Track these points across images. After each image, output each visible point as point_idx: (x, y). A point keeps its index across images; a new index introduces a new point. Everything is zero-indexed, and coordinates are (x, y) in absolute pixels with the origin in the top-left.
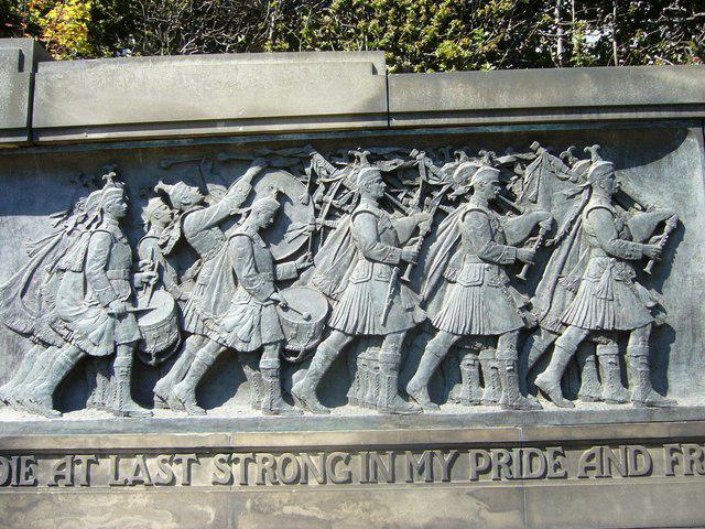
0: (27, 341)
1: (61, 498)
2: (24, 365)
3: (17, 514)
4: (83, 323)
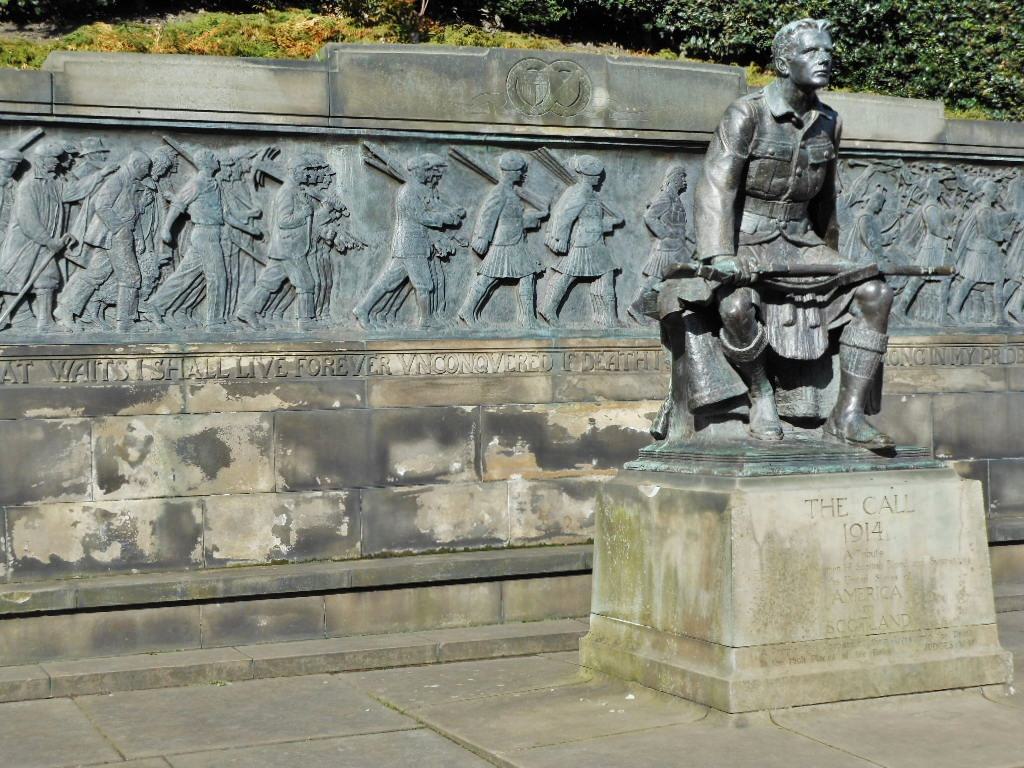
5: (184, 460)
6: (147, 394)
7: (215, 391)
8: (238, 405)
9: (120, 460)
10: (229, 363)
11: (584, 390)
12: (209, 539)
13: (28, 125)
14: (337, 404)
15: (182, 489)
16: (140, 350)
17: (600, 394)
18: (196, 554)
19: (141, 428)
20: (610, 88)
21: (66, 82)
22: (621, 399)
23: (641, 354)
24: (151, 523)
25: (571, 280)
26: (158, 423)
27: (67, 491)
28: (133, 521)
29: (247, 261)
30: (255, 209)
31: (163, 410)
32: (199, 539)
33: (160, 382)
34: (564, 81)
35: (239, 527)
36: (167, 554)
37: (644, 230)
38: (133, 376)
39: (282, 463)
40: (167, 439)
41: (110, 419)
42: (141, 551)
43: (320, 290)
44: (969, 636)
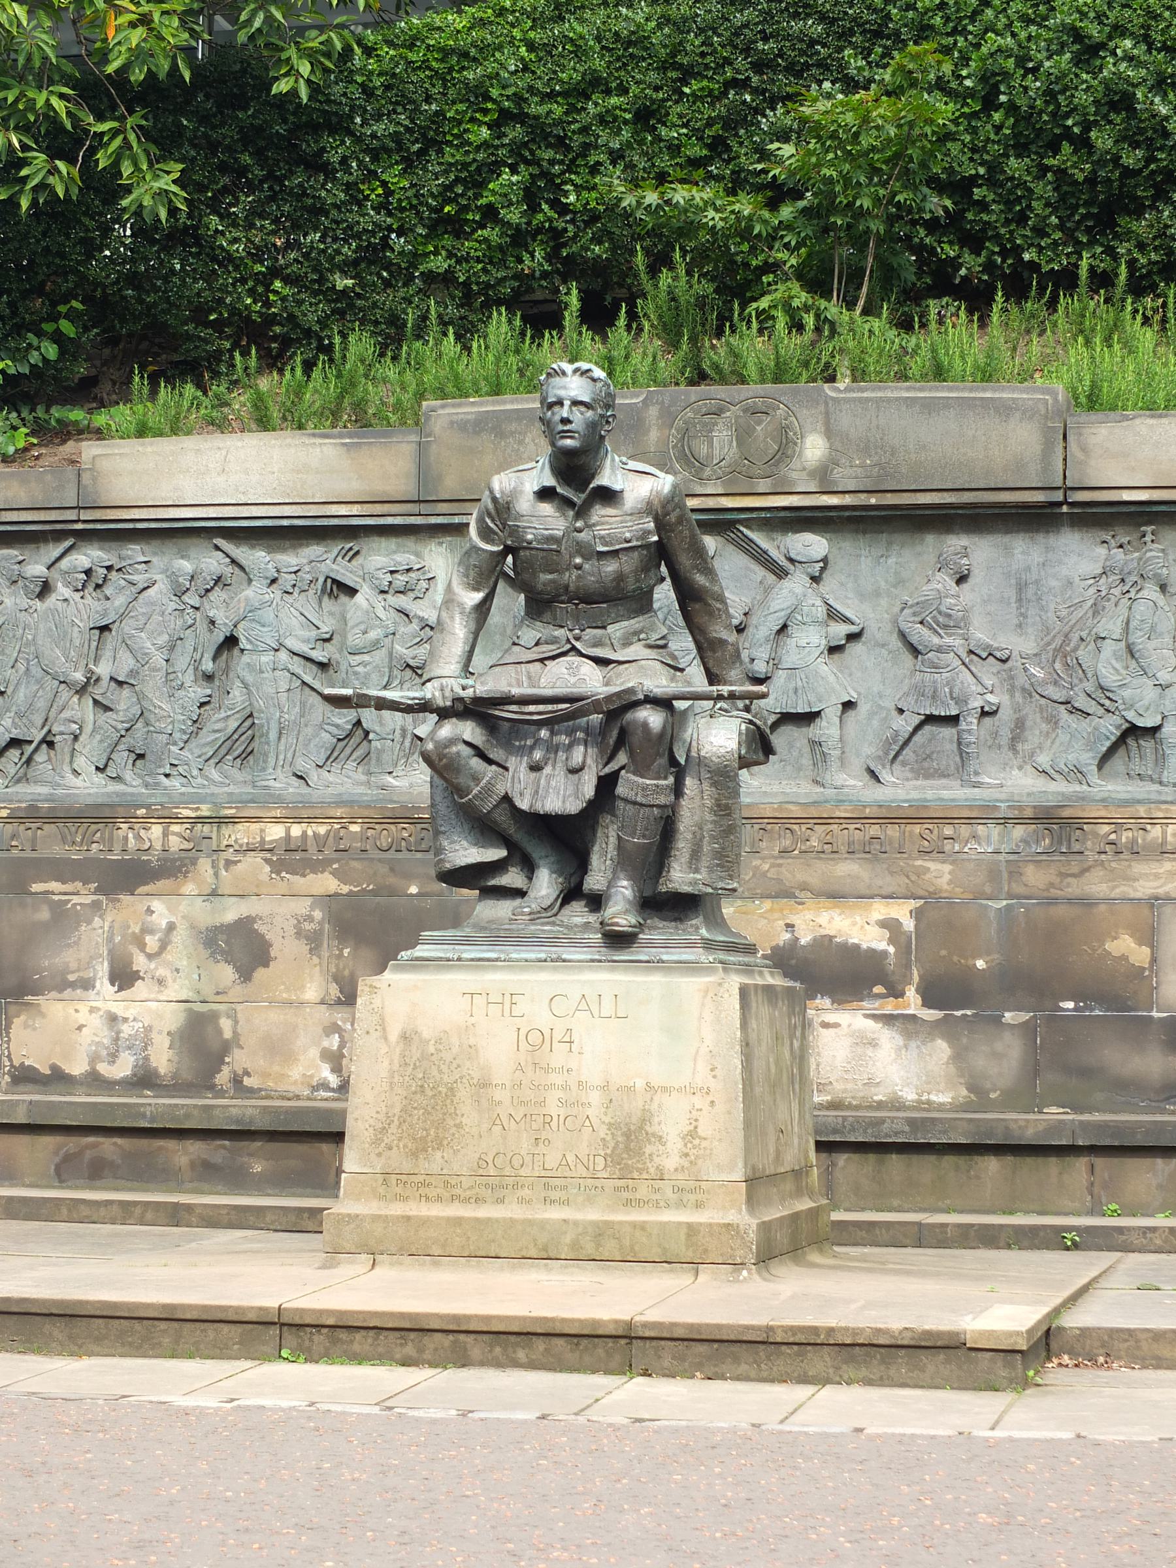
0: (1063, 707)
1: (1114, 865)
2: (1063, 737)
3: (1070, 880)
4: (1127, 693)
5: (212, 955)
6: (171, 868)
7: (254, 864)
8: (282, 887)
9: (135, 950)
10: (275, 832)
11: (779, 881)
12: (238, 1059)
13: (58, 536)
14: (413, 890)
15: (208, 991)
16: (166, 814)
17: (804, 887)
18: (223, 1078)
19: (161, 912)
20: (829, 433)
21: (94, 479)
22: (835, 895)
23: (874, 830)
24: (169, 1033)
26: (184, 906)
27: (73, 985)
28: (148, 1029)
29: (315, 699)
30: (324, 629)
31: (189, 888)
32: (227, 1060)
33: (190, 854)
34: (759, 428)
35: (279, 1048)
36: (187, 1075)
37: (895, 643)
38: (158, 846)
39: (337, 966)
40: (192, 927)
41: (125, 898)
42: (156, 1069)
43: (404, 736)
44: (692, 1191)
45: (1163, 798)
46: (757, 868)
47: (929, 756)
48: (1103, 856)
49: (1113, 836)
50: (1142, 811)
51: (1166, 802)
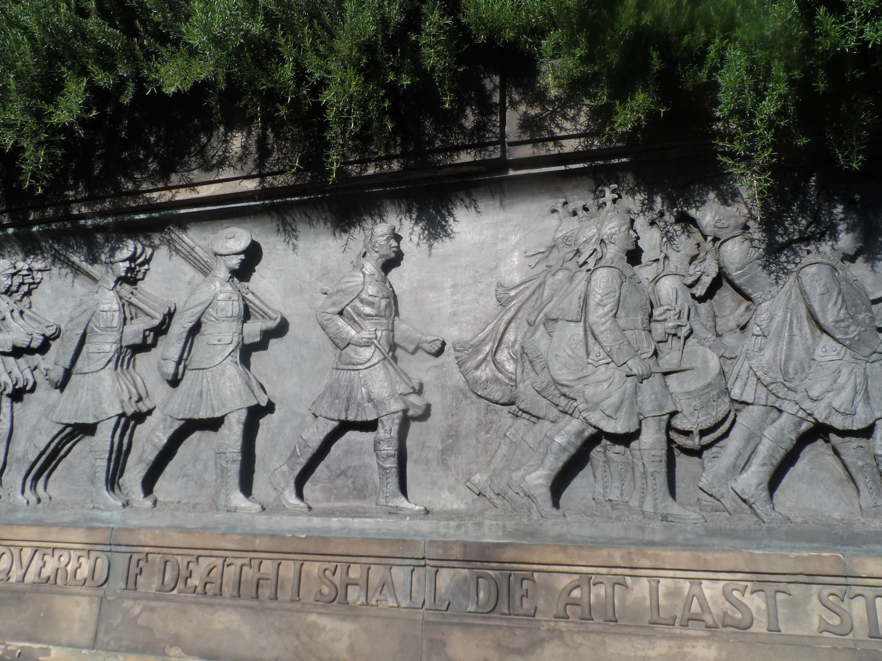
1: (578, 639)
17: (176, 641)
25: (177, 425)
45: (648, 537)
46: (128, 611)
47: (343, 473)
48: (562, 625)
49: (576, 593)
50: (618, 557)
51: (652, 544)
